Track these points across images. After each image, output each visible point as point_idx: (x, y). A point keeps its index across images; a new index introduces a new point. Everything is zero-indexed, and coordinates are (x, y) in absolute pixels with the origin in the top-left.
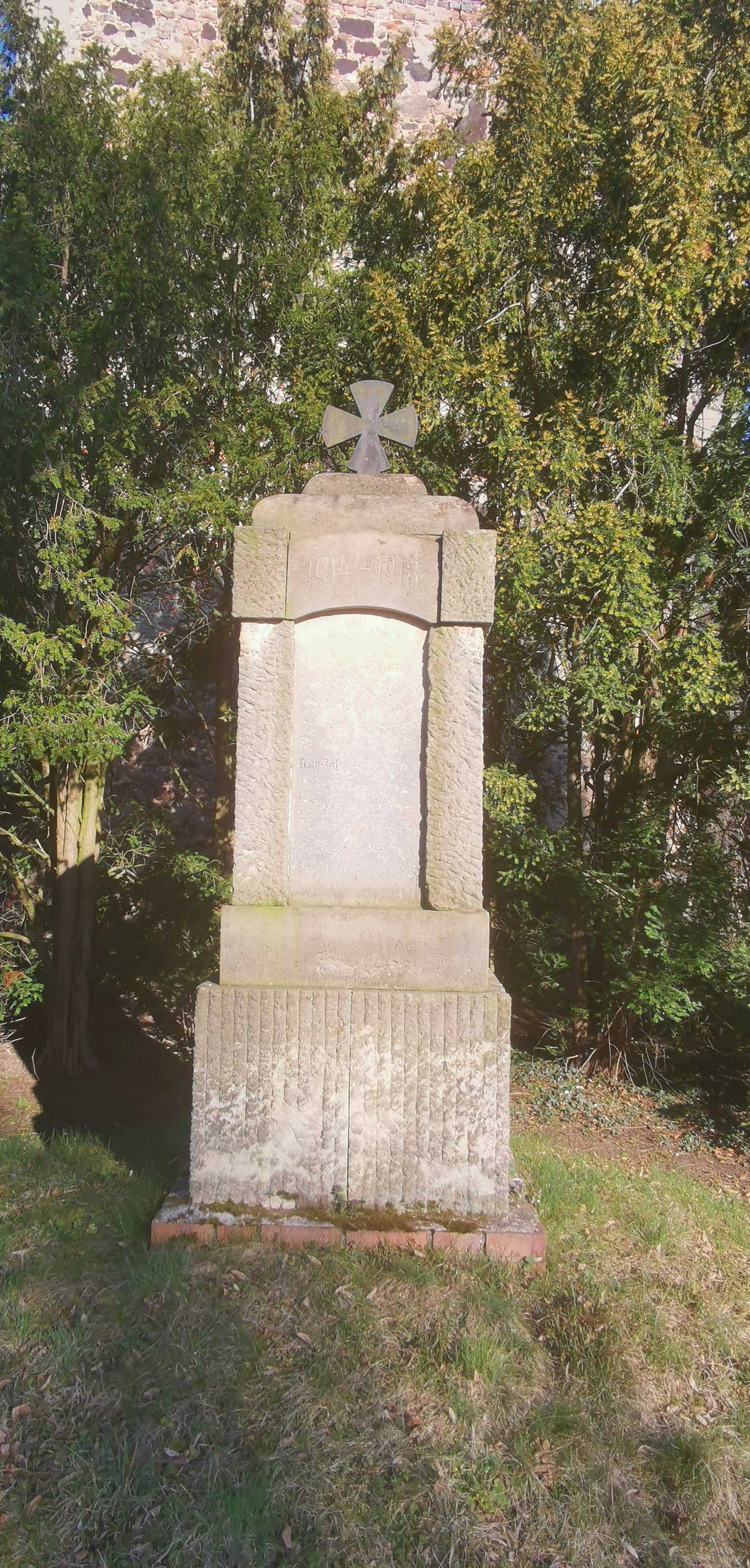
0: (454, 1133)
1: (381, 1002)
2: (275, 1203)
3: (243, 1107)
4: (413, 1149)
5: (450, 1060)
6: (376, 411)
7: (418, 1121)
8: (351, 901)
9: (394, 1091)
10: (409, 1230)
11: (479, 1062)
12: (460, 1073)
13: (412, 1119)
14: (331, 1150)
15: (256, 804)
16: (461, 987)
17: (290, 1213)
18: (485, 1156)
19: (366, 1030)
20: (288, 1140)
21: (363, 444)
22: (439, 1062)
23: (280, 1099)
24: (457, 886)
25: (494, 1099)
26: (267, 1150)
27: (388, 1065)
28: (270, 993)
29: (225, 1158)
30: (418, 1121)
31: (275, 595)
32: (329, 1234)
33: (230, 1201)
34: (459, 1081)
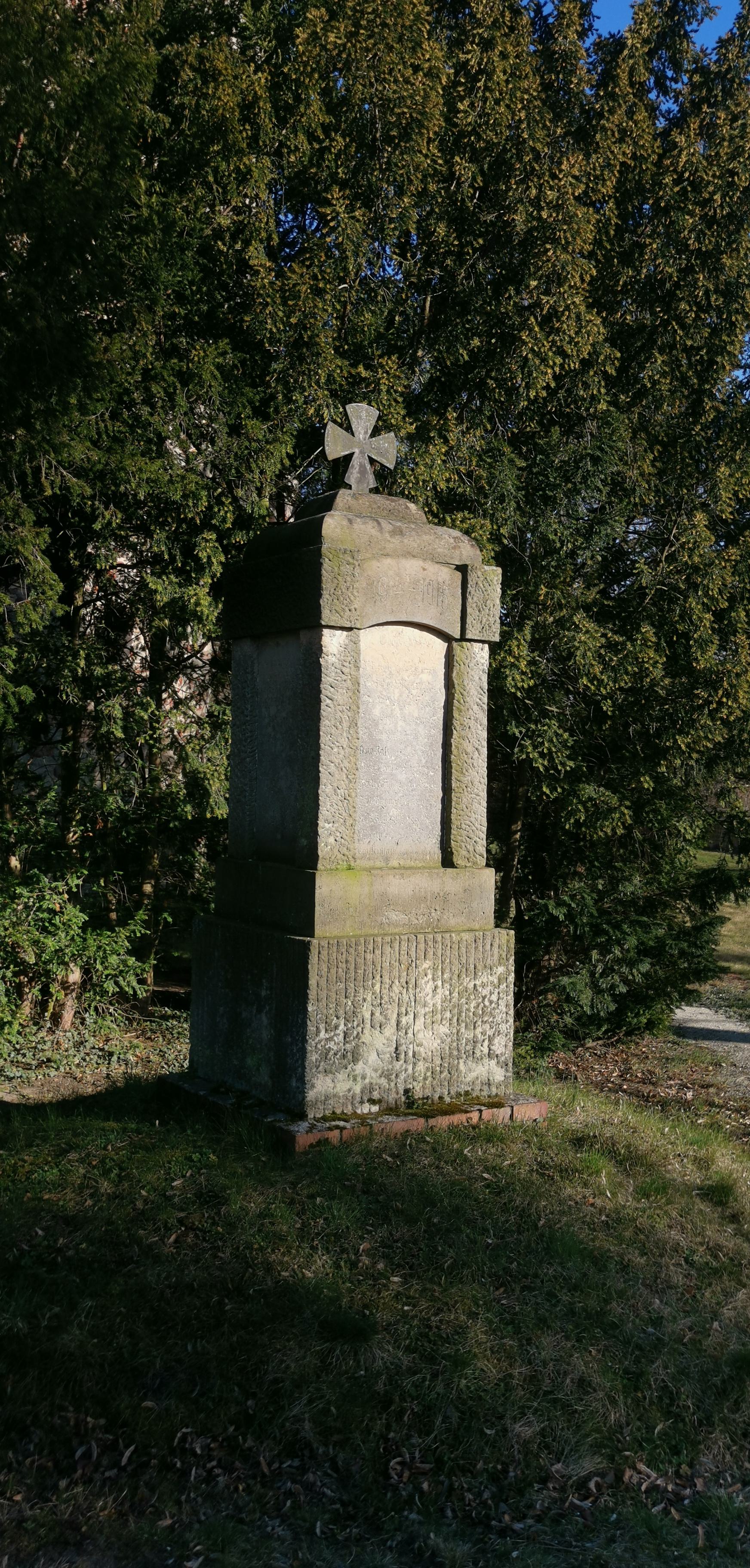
0: (480, 1037)
1: (435, 941)
2: (366, 1108)
3: (342, 1035)
4: (455, 1053)
5: (478, 983)
6: (366, 433)
7: (458, 1032)
8: (394, 863)
9: (444, 1010)
10: (466, 1112)
11: (496, 981)
12: (485, 992)
13: (455, 1031)
14: (402, 1062)
15: (335, 785)
16: (477, 927)
17: (378, 1114)
18: (498, 1052)
19: (427, 964)
20: (373, 1057)
21: (355, 462)
22: (471, 985)
23: (368, 1026)
24: (471, 849)
25: (504, 1010)
26: (359, 1067)
27: (439, 990)
28: (380, 939)
29: (328, 1080)
30: (458, 1032)
31: (352, 608)
32: (418, 1124)
33: (334, 1113)
34: (484, 998)
